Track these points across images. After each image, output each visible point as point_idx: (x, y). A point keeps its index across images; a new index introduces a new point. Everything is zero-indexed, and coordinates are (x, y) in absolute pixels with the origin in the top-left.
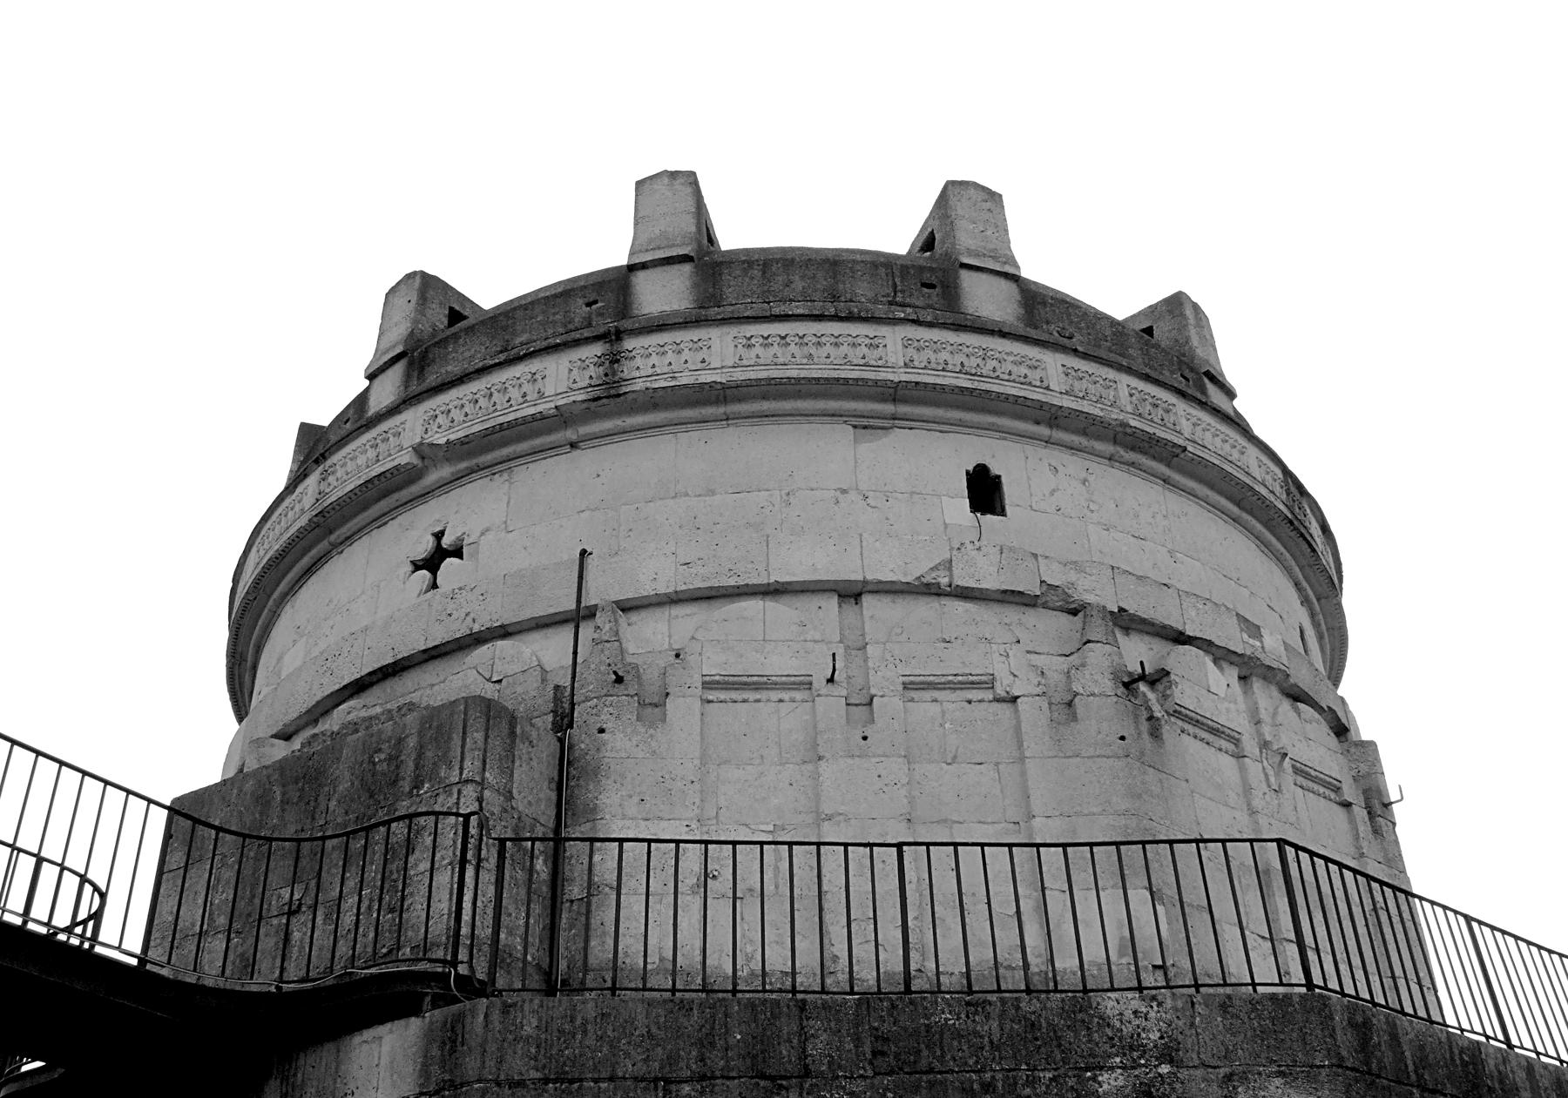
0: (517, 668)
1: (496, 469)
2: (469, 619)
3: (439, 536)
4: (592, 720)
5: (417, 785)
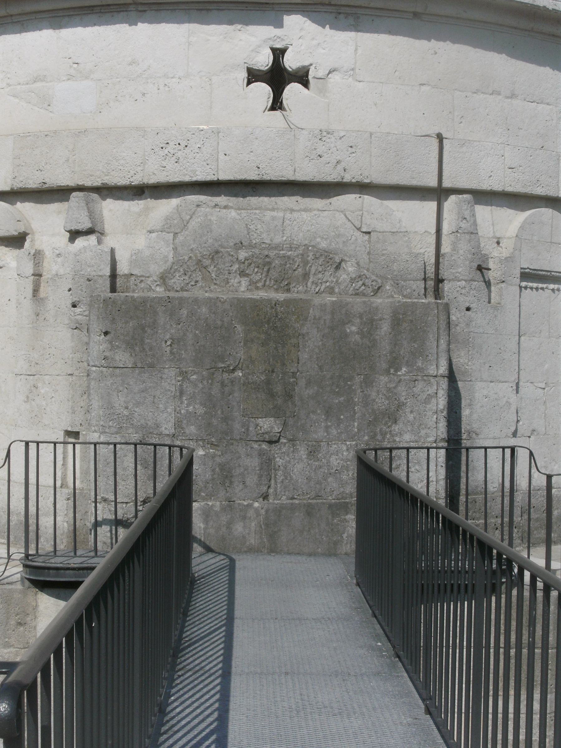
0: (386, 227)
1: (343, 10)
2: (340, 167)
3: (278, 54)
4: (461, 298)
5: (394, 363)
